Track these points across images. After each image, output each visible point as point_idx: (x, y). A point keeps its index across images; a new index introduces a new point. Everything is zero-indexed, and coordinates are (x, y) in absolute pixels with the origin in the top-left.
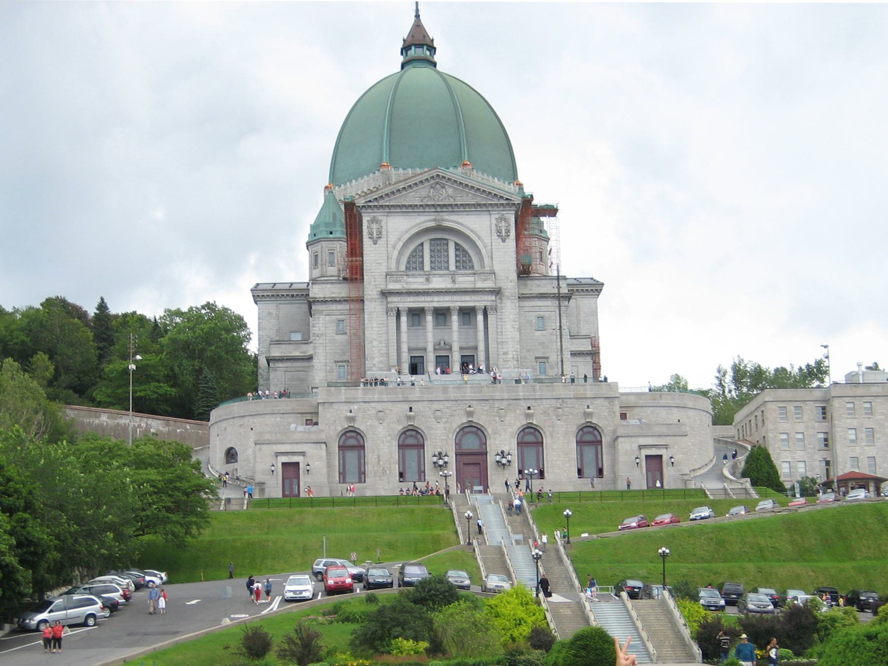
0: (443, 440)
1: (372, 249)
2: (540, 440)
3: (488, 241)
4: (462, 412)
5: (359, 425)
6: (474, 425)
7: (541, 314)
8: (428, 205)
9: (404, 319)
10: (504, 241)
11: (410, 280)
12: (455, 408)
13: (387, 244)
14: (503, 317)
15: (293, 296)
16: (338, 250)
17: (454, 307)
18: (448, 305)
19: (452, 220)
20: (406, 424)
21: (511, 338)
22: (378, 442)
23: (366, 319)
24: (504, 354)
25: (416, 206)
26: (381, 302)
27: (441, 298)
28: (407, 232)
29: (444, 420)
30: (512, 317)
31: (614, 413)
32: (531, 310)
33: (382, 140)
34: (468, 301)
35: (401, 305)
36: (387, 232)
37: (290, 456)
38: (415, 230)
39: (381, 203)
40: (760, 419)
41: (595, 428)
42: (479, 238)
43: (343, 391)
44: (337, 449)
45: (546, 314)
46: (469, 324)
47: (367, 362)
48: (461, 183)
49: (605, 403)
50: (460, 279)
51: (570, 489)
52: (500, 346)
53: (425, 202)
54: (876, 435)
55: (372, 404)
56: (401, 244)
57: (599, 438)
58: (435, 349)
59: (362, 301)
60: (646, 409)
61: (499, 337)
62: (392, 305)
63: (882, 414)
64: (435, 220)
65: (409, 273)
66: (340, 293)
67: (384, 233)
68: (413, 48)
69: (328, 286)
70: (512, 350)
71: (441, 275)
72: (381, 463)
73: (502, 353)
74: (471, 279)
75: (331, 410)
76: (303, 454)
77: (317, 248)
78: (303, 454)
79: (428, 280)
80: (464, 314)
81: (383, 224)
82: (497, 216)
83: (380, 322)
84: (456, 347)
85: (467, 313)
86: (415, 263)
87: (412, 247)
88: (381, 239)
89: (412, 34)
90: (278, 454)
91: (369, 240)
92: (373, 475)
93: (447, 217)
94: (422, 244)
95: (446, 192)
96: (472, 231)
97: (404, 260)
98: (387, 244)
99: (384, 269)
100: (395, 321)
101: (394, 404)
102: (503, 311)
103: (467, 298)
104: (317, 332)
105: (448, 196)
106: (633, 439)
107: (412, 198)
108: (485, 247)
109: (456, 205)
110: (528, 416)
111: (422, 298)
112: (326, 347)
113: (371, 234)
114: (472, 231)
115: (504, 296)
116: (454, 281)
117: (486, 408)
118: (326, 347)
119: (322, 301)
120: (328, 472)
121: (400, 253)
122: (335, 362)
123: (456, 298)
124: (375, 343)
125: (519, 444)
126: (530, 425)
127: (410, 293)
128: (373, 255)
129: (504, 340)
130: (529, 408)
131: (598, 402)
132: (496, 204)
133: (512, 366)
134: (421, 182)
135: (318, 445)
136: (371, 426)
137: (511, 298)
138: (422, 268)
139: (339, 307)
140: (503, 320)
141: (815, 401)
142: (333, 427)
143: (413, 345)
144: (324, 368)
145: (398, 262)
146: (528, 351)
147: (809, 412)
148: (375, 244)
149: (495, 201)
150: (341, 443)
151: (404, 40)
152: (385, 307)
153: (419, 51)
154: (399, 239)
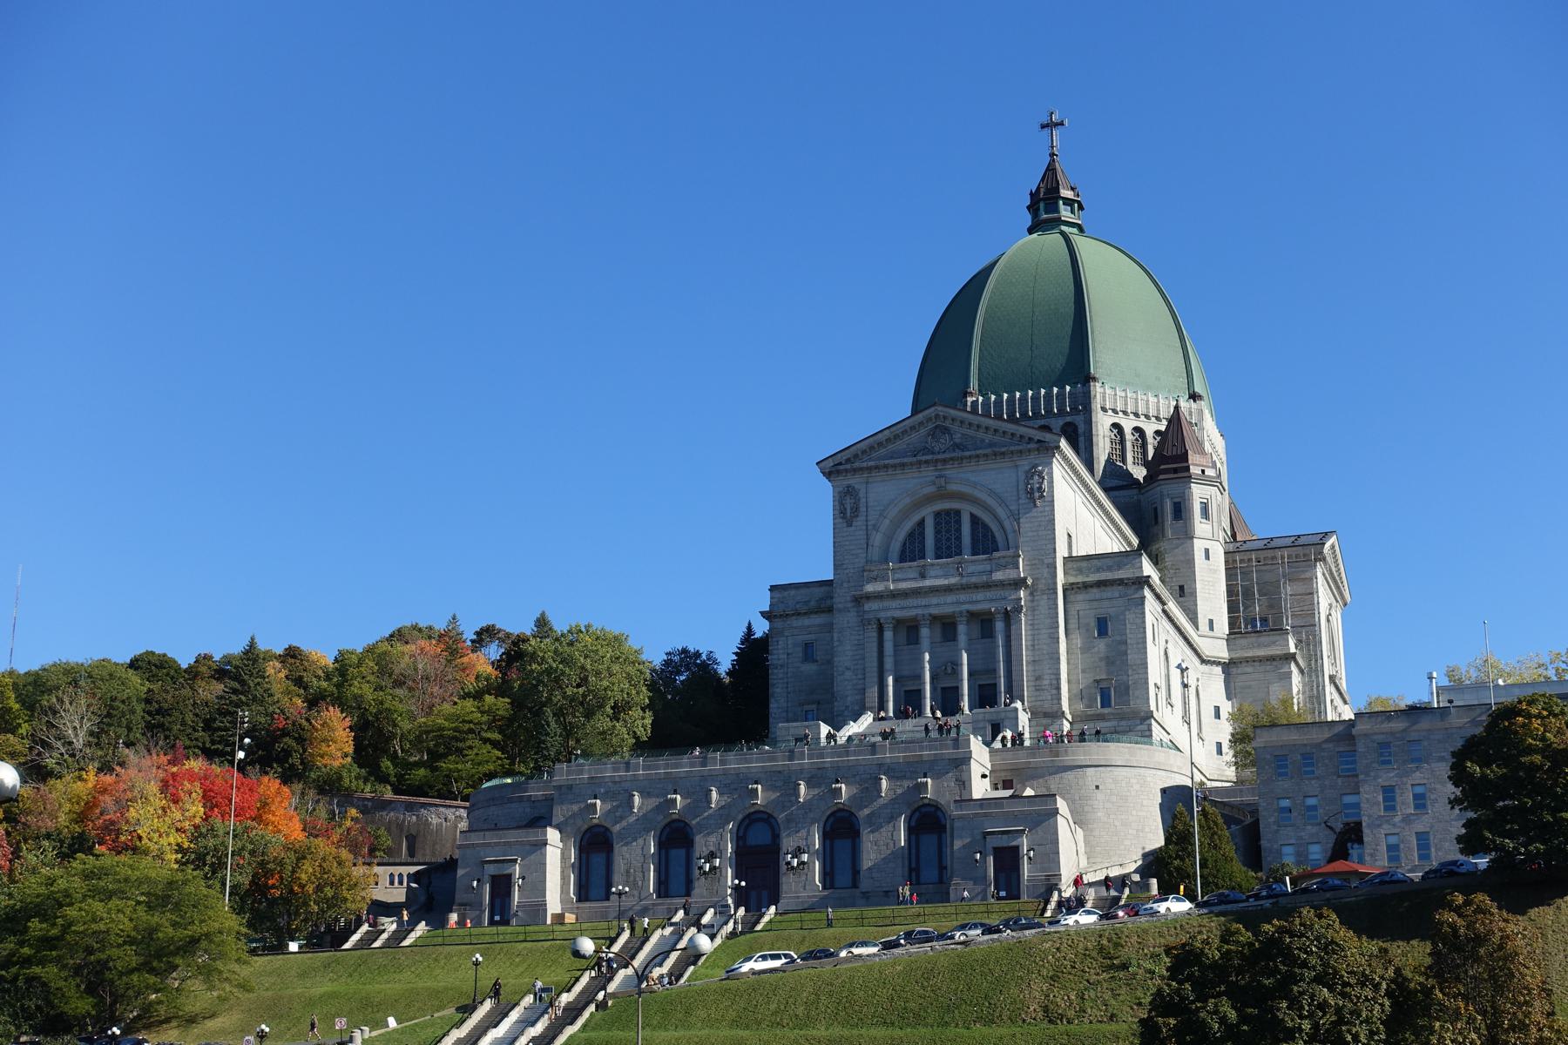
1: (845, 534)
8: (920, 463)
9: (888, 635)
13: (867, 526)
14: (1036, 622)
17: (961, 612)
21: (1048, 654)
23: (835, 639)
24: (1036, 680)
26: (857, 612)
27: (941, 599)
30: (1048, 621)
32: (1088, 607)
34: (983, 602)
35: (882, 615)
36: (867, 507)
38: (908, 500)
39: (857, 465)
45: (1112, 611)
47: (835, 704)
66: (809, 601)
67: (863, 509)
68: (1042, 205)
70: (1050, 671)
72: (632, 871)
73: (1032, 679)
83: (856, 642)
85: (984, 623)
86: (912, 550)
87: (908, 525)
91: (841, 520)
94: (921, 523)
95: (952, 439)
97: (896, 547)
98: (867, 526)
100: (875, 639)
102: (1036, 613)
103: (980, 596)
104: (775, 662)
112: (787, 683)
115: (1036, 590)
118: (787, 683)
119: (781, 615)
121: (890, 538)
122: (801, 705)
123: (963, 597)
124: (848, 674)
127: (894, 595)
128: (847, 543)
129: (1037, 658)
133: (1049, 697)
137: (1047, 592)
139: (806, 621)
140: (1036, 627)
144: (784, 714)
147: (1326, 761)
148: (850, 525)
151: (1031, 194)
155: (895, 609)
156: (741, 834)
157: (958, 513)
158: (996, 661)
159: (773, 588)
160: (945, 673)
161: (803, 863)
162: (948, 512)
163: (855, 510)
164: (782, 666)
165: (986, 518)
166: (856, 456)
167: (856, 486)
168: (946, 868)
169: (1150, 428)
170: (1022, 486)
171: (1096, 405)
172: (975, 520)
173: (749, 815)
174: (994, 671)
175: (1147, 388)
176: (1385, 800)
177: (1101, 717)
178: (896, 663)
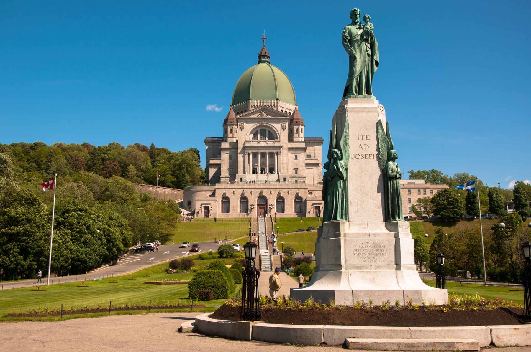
3: (279, 130)
9: (251, 156)
10: (284, 130)
15: (218, 143)
35: (250, 151)
42: (276, 129)
49: (304, 190)
50: (269, 143)
51: (292, 216)
65: (253, 140)
78: (210, 204)
94: (258, 131)
116: (267, 143)
124: (241, 163)
125: (277, 202)
130: (280, 191)
138: (257, 139)
146: (291, 166)
157: (265, 130)
158: (274, 163)
160: (263, 164)
161: (273, 207)
162: (263, 129)
164: (224, 160)
165: (272, 132)
169: (288, 111)
171: (279, 105)
172: (269, 132)
174: (274, 165)
175: (287, 102)
177: (295, 177)
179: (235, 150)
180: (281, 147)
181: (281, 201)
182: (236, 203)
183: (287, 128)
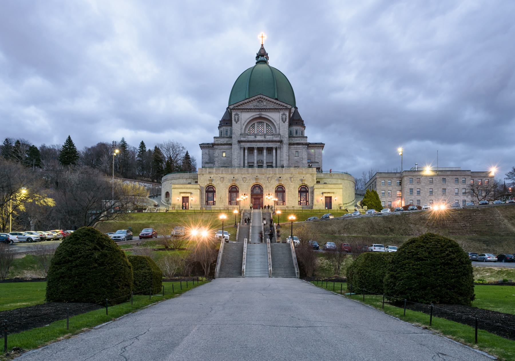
0: (246, 189)
2: (284, 190)
4: (254, 179)
5: (214, 183)
6: (258, 184)
7: (297, 150)
8: (256, 109)
9: (246, 151)
10: (284, 123)
11: (249, 137)
12: (250, 177)
16: (229, 129)
17: (265, 147)
18: (262, 146)
19: (265, 114)
20: (232, 183)
22: (221, 190)
25: (252, 109)
28: (248, 119)
29: (247, 182)
30: (286, 151)
31: (314, 180)
33: (246, 90)
34: (270, 145)
35: (245, 146)
37: (185, 194)
38: (251, 118)
39: (239, 107)
40: (374, 185)
41: (306, 186)
42: (275, 121)
43: (208, 170)
44: (205, 192)
45: (299, 151)
46: (271, 154)
48: (269, 100)
49: (311, 176)
50: (267, 137)
52: (281, 162)
53: (255, 107)
54: (421, 192)
55: (219, 175)
56: (246, 123)
57: (307, 190)
58: (257, 163)
59: (232, 145)
60: (327, 179)
61: (281, 158)
62: (242, 146)
63: (425, 183)
64: (259, 114)
67: (240, 119)
69: (220, 139)
71: (260, 135)
74: (272, 137)
75: (203, 177)
76: (191, 193)
77: (222, 129)
79: (255, 137)
80: (269, 150)
81: (240, 116)
82: (282, 113)
84: (265, 162)
85: (269, 150)
88: (239, 121)
89: (260, 52)
90: (181, 193)
92: (218, 202)
93: (264, 113)
96: (272, 119)
99: (240, 133)
101: (227, 175)
103: (270, 144)
105: (264, 105)
106: (320, 190)
107: (251, 106)
108: (277, 125)
109: (267, 109)
110: (279, 180)
111: (253, 144)
113: (235, 119)
114: (272, 119)
116: (265, 138)
117: (263, 177)
120: (201, 201)
123: (265, 144)
124: (236, 160)
126: (280, 184)
130: (280, 177)
131: (308, 175)
132: (282, 109)
134: (254, 100)
135: (196, 190)
136: (218, 184)
139: (223, 147)
141: (397, 178)
142: (203, 184)
143: (249, 161)
145: (245, 130)
146: (292, 164)
149: (281, 107)
150: (207, 190)
152: (239, 147)
153: (262, 58)
154: (245, 122)
155: (248, 145)
156: (252, 190)
159: (215, 138)
163: (238, 119)
164: (217, 157)
166: (239, 105)
167: (239, 113)
168: (308, 201)
170: (281, 117)
173: (254, 186)
176: (410, 192)
178: (248, 158)
179: (230, 147)
180: (281, 142)
181: (280, 191)
182: (224, 193)
183: (287, 120)
